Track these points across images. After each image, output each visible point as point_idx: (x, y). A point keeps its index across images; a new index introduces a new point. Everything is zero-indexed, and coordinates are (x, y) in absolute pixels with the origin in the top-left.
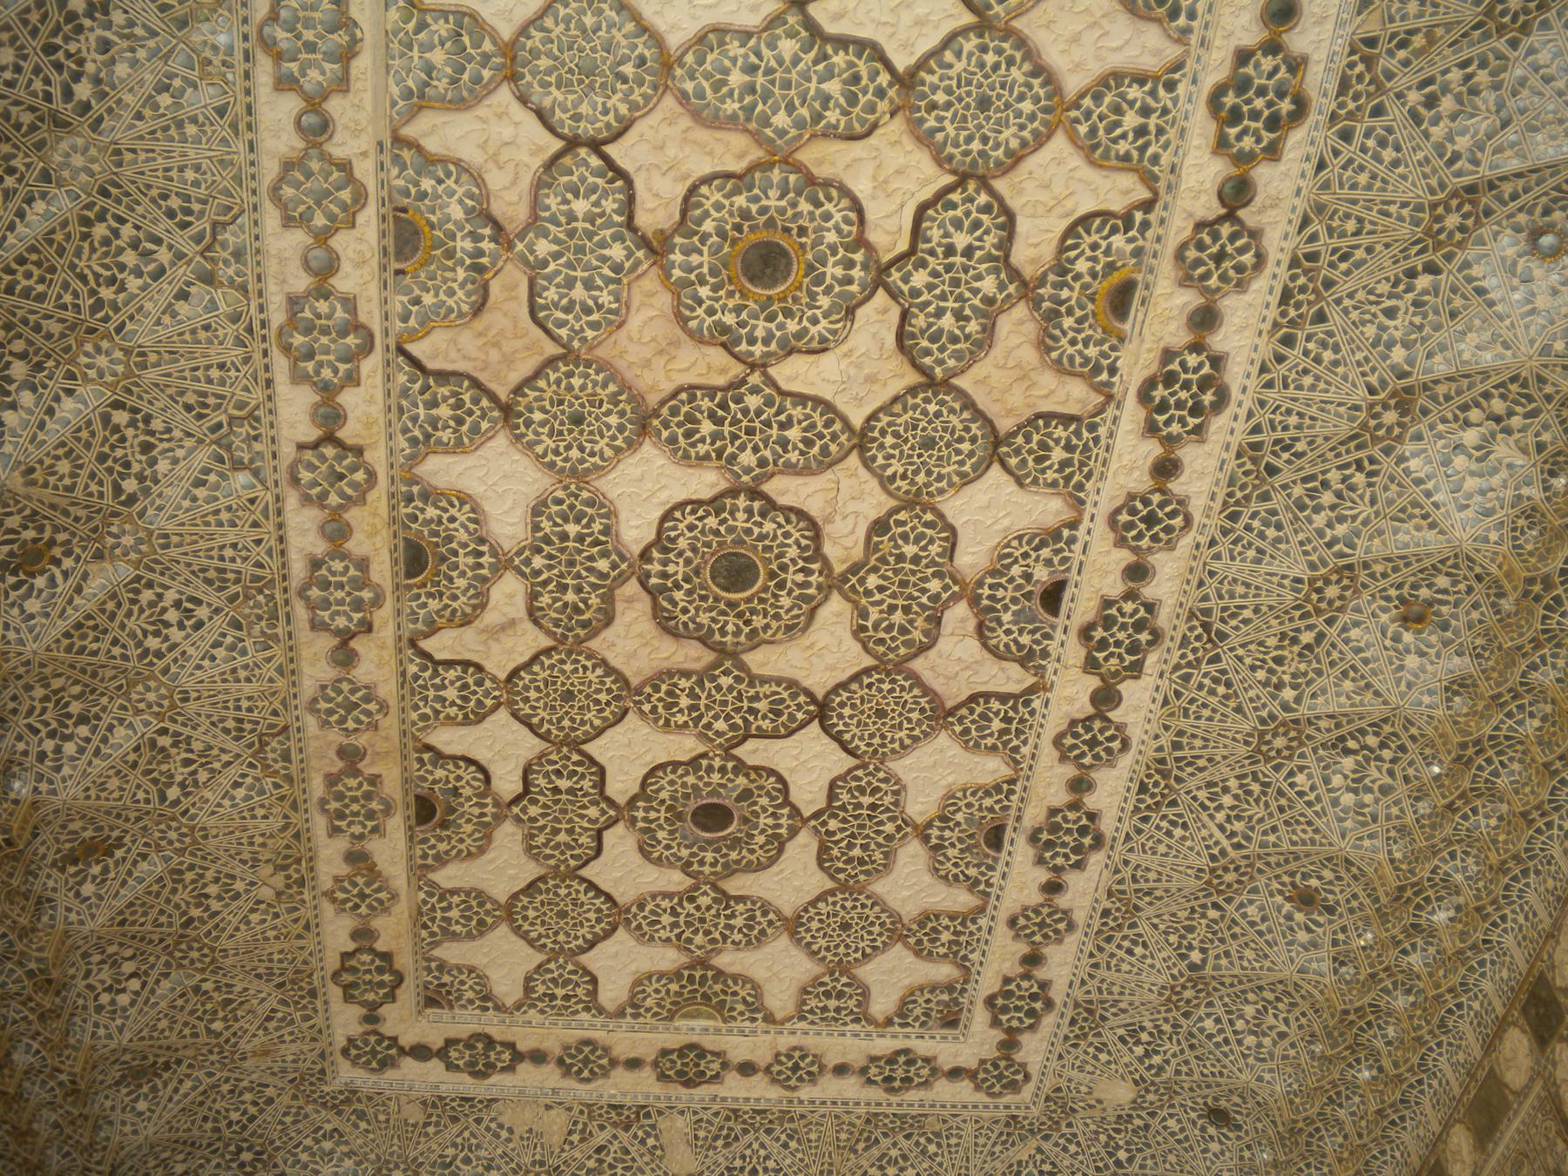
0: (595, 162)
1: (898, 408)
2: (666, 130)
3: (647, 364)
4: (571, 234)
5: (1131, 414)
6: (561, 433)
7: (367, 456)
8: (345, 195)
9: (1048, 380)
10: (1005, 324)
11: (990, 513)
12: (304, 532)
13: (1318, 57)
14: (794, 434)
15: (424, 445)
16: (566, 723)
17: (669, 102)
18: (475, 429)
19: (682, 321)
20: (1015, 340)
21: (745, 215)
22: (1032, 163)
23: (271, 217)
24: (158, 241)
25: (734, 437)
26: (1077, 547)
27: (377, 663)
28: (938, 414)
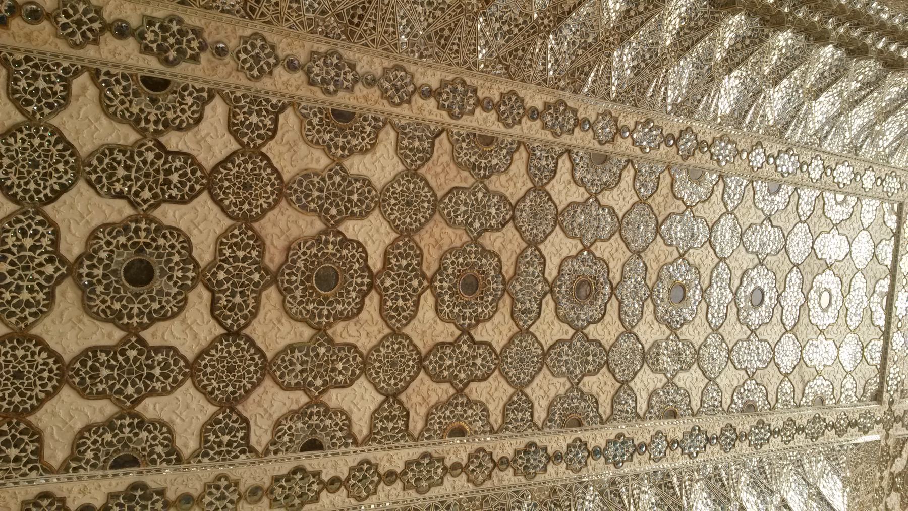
0: (508, 217)
1: (411, 348)
2: (516, 244)
3: (431, 235)
4: (484, 206)
5: (414, 453)
6: (403, 196)
7: (405, 105)
8: (510, 121)
9: (423, 411)
10: (446, 386)
11: (359, 401)
12: (370, 62)
13: (547, 476)
14: (400, 302)
15: (401, 131)
16: (226, 184)
17: (524, 245)
18: (406, 156)
19: (450, 251)
20: (440, 392)
21: (487, 275)
22: (504, 382)
23: (505, 89)
24: (507, 42)
25: (399, 275)
26: (343, 449)
27: (283, 82)
28: (408, 366)
